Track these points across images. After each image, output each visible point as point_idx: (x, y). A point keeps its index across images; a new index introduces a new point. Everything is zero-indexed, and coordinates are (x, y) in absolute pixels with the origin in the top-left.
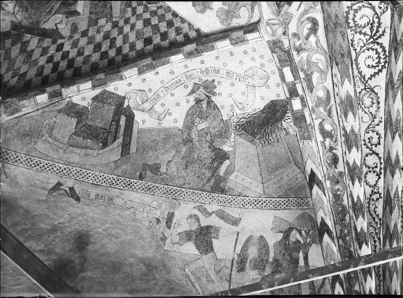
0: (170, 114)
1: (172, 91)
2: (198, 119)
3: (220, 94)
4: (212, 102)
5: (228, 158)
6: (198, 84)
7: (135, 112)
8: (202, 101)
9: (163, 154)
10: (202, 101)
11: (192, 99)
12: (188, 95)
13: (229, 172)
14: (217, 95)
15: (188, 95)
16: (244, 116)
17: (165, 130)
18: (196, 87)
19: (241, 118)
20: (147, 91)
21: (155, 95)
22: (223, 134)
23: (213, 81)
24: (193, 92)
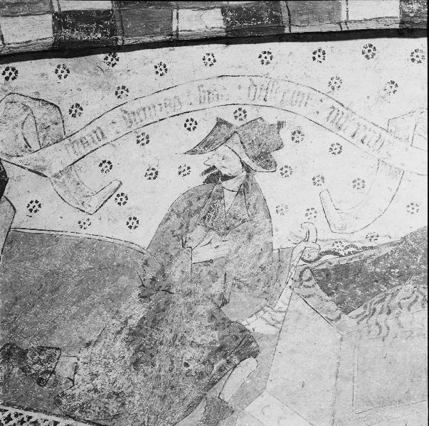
0: (122, 199)
1: (144, 130)
2: (200, 231)
3: (286, 172)
4: (257, 188)
5: (254, 355)
6: (230, 126)
7: (12, 172)
8: (226, 178)
9: (73, 317)
10: (226, 178)
11: (199, 164)
12: (193, 152)
13: (246, 395)
14: (278, 171)
15: (193, 152)
16: (338, 247)
17: (97, 244)
18: (222, 131)
19: (327, 253)
20: (65, 109)
21: (90, 129)
22: (264, 283)
23: (280, 125)
24: (207, 144)
